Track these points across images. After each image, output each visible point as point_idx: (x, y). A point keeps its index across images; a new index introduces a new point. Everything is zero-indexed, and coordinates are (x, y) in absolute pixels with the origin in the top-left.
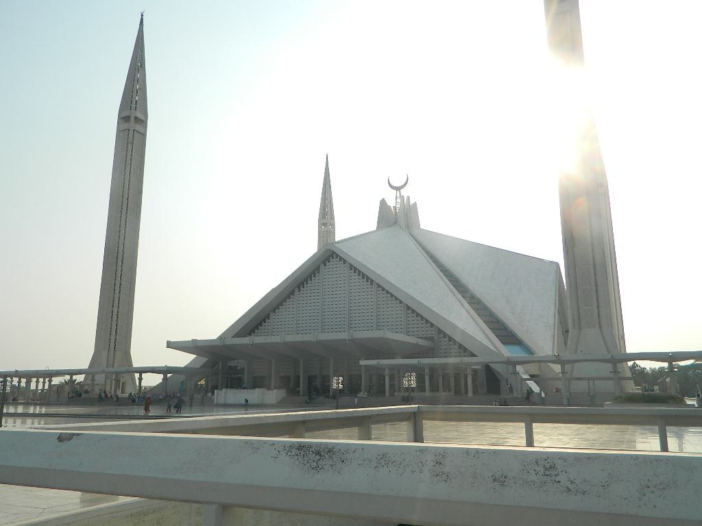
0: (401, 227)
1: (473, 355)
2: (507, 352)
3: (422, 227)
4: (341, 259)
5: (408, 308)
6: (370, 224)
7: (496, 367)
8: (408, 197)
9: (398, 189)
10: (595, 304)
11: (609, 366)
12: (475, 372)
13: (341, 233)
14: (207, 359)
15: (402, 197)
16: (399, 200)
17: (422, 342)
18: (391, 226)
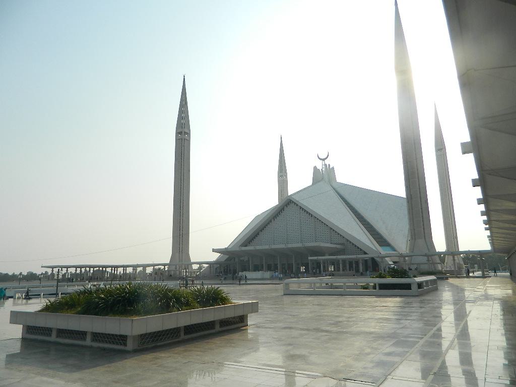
1: (365, 253)
2: (383, 251)
3: (338, 180)
4: (295, 203)
5: (331, 229)
7: (378, 259)
8: (329, 165)
9: (323, 160)
10: (422, 227)
11: (426, 258)
12: (366, 261)
13: (293, 188)
14: (227, 257)
15: (326, 165)
16: (324, 166)
17: (338, 246)
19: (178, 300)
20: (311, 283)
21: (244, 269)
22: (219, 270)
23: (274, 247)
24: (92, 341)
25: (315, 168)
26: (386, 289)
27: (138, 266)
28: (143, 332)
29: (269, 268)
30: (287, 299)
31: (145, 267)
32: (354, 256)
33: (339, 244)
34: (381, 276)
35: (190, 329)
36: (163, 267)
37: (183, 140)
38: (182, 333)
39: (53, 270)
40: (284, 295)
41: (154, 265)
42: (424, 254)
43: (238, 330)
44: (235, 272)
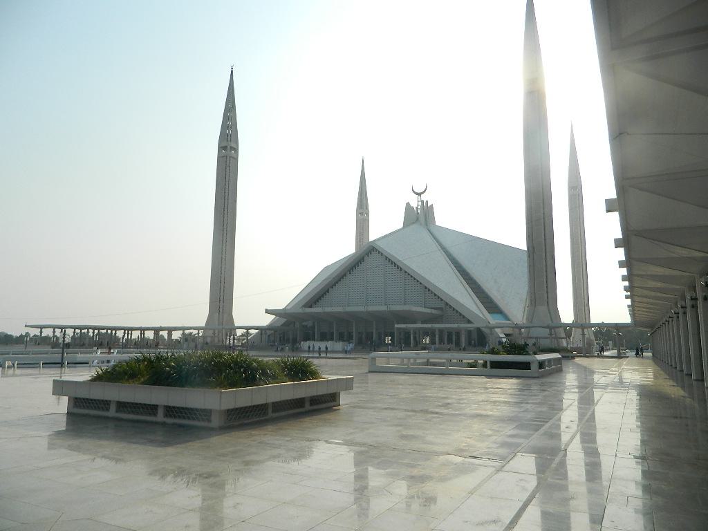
0: (421, 224)
1: (469, 322)
2: (493, 320)
3: (437, 224)
4: (379, 252)
5: (426, 288)
6: (397, 222)
8: (427, 202)
9: (419, 194)
11: (548, 330)
12: (469, 332)
13: (376, 232)
15: (423, 202)
16: (420, 203)
17: (434, 311)
18: (413, 223)
19: (264, 373)
20: (402, 359)
21: (305, 340)
22: (272, 338)
23: (349, 309)
24: (164, 417)
25: (408, 204)
26: (499, 368)
27: (176, 329)
28: (231, 407)
29: (341, 338)
30: (371, 376)
31: (170, 330)
32: (455, 326)
33: (434, 309)
34: (493, 352)
35: (278, 406)
36: (196, 332)
37: (228, 157)
38: (270, 410)
39: (54, 330)
40: (370, 372)
41: (183, 329)
42: (545, 325)
43: (329, 409)
44: (295, 341)
